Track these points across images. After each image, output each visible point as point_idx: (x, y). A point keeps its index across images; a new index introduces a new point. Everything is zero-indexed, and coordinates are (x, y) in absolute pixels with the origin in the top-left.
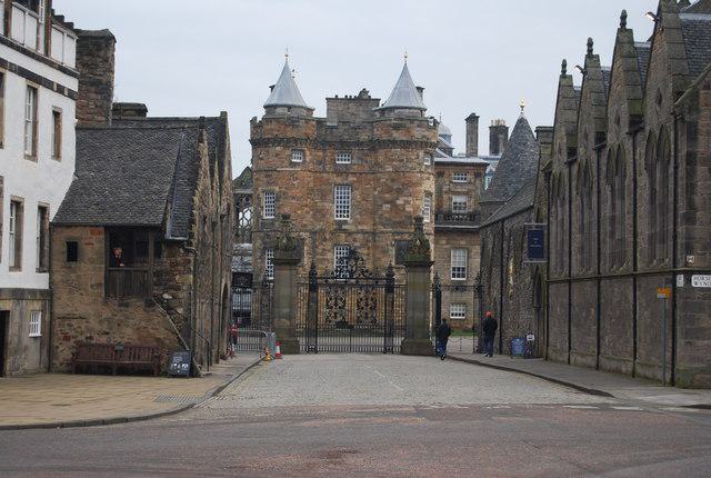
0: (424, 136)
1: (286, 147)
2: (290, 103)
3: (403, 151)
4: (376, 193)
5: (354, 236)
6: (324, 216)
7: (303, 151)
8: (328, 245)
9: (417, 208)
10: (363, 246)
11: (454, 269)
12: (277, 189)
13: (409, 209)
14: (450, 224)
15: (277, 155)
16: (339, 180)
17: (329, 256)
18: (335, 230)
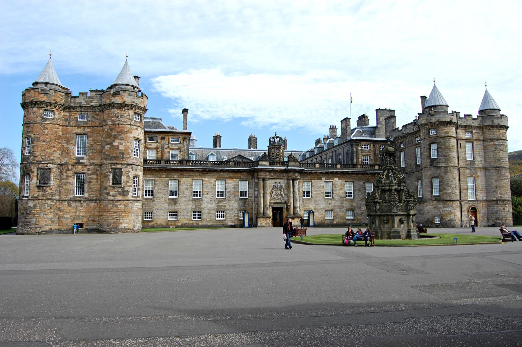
0: (134, 102)
1: (39, 108)
2: (47, 81)
3: (119, 111)
4: (103, 139)
5: (88, 167)
6: (68, 154)
7: (53, 111)
8: (71, 173)
9: (127, 148)
10: (94, 173)
11: (170, 191)
12: (33, 135)
13: (121, 148)
14: (168, 166)
15: (34, 113)
16: (79, 131)
17: (70, 180)
18: (75, 163)
